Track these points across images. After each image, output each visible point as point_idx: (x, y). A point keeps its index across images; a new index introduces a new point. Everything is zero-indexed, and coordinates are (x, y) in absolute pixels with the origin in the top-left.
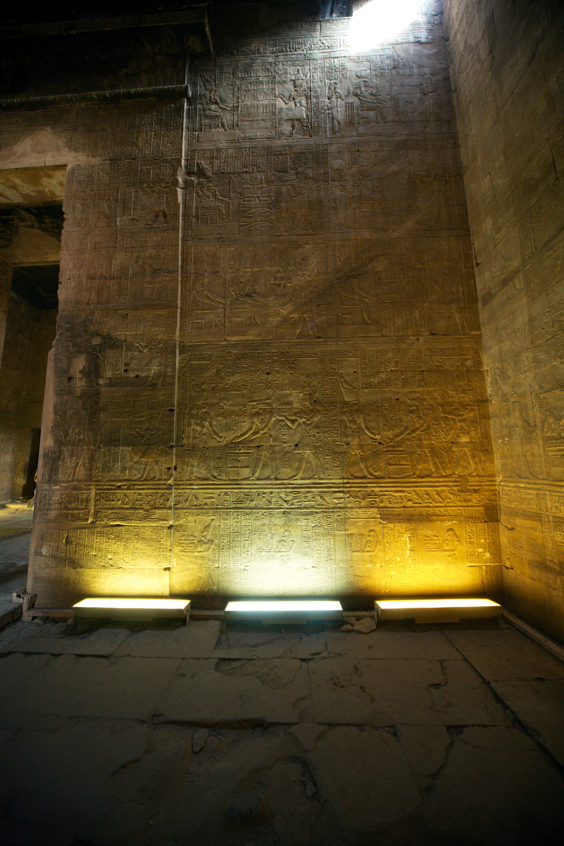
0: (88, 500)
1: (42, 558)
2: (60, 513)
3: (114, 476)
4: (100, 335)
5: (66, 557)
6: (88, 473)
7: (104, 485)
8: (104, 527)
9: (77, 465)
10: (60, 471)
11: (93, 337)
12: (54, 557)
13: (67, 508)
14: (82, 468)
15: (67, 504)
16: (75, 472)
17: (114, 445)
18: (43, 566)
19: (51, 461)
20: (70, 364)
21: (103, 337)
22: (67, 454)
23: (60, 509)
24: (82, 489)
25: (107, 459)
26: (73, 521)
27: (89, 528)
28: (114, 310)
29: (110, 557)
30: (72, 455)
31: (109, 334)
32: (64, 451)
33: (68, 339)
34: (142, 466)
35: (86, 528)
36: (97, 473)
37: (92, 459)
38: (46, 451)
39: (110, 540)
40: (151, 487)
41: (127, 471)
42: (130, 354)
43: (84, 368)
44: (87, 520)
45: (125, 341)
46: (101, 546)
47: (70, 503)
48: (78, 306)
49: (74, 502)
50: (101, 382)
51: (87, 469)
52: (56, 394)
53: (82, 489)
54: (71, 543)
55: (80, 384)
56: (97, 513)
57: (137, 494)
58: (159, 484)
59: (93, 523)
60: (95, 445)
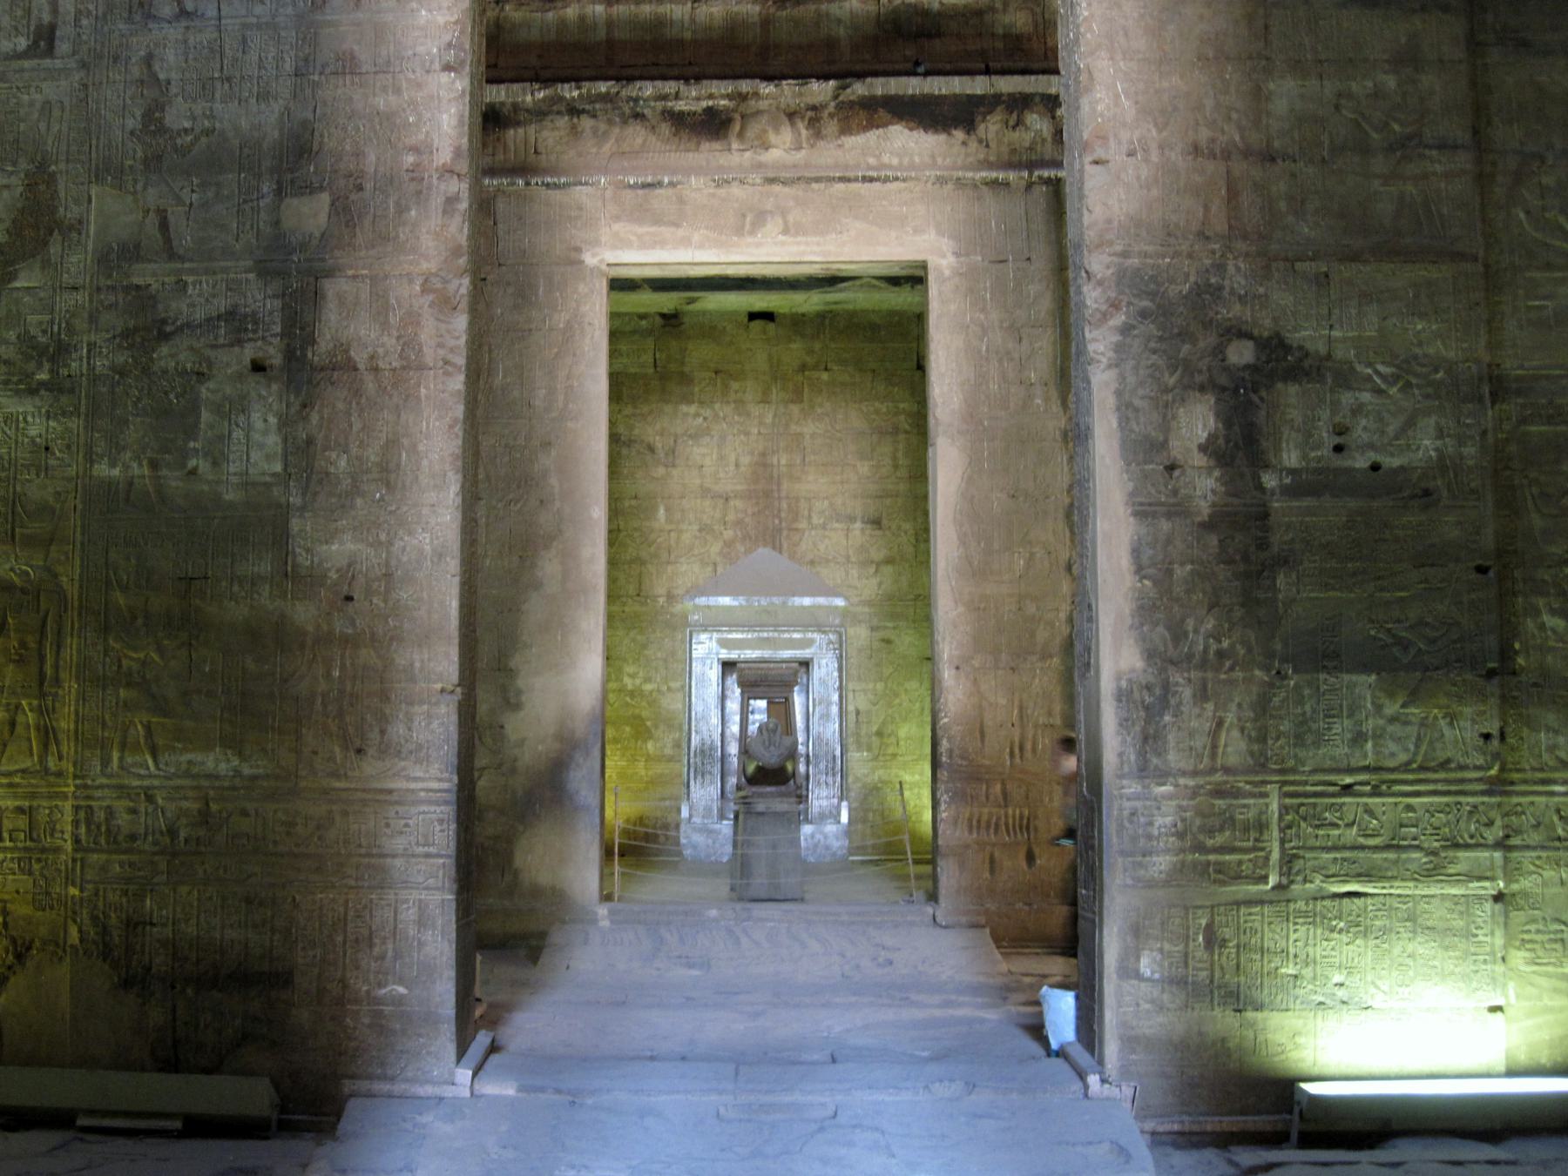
0: (1262, 826)
1: (1143, 985)
2: (1183, 863)
3: (1333, 758)
4: (1249, 336)
5: (1212, 981)
6: (1256, 747)
7: (1306, 783)
8: (1315, 899)
9: (1220, 724)
10: (1172, 744)
11: (1230, 340)
12: (1179, 982)
13: (1200, 848)
14: (1236, 733)
15: (1201, 837)
16: (1214, 747)
17: (1324, 667)
18: (1147, 1006)
19: (1142, 714)
20: (1166, 426)
21: (1263, 345)
22: (1187, 693)
23: (1182, 851)
24: (1237, 794)
25: (1308, 708)
26: (1223, 883)
27: (1271, 902)
28: (1286, 259)
29: (1338, 978)
30: (1202, 695)
31: (1278, 335)
32: (1177, 684)
33: (1152, 345)
34: (1413, 730)
35: (1262, 902)
36: (1282, 747)
37: (1262, 707)
38: (1124, 684)
39: (1335, 935)
40: (1440, 787)
41: (1369, 745)
42: (1347, 398)
43: (1212, 438)
44: (1265, 879)
45: (1329, 357)
46: (1310, 950)
47: (1211, 832)
48: (1172, 240)
49: (1222, 829)
50: (1270, 481)
51: (1250, 737)
52: (1136, 514)
53: (1237, 794)
54: (1224, 943)
55: (1204, 487)
56: (1288, 861)
57: (1400, 807)
58: (1462, 781)
59: (1279, 887)
60: (1267, 669)
